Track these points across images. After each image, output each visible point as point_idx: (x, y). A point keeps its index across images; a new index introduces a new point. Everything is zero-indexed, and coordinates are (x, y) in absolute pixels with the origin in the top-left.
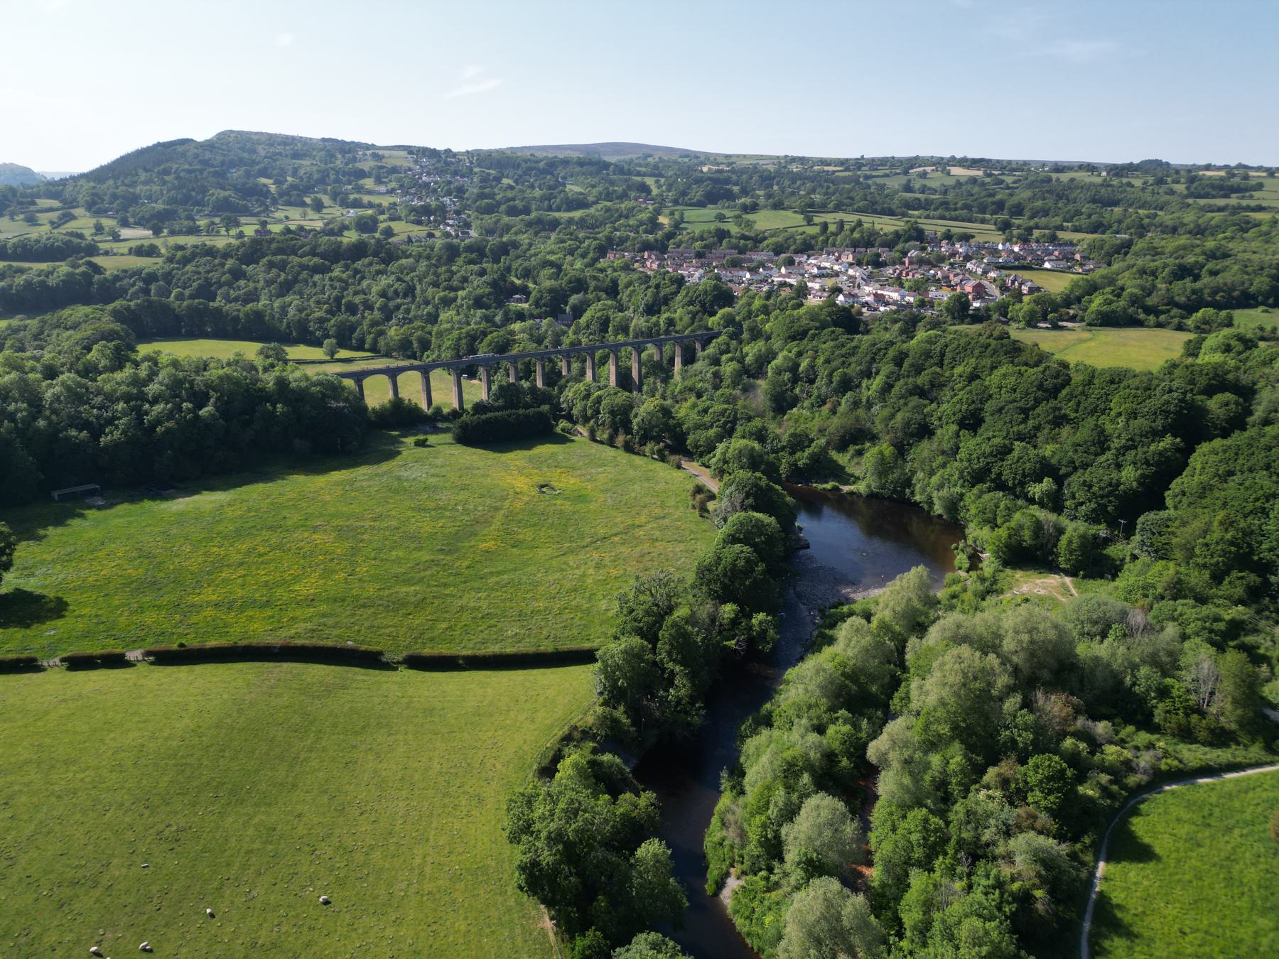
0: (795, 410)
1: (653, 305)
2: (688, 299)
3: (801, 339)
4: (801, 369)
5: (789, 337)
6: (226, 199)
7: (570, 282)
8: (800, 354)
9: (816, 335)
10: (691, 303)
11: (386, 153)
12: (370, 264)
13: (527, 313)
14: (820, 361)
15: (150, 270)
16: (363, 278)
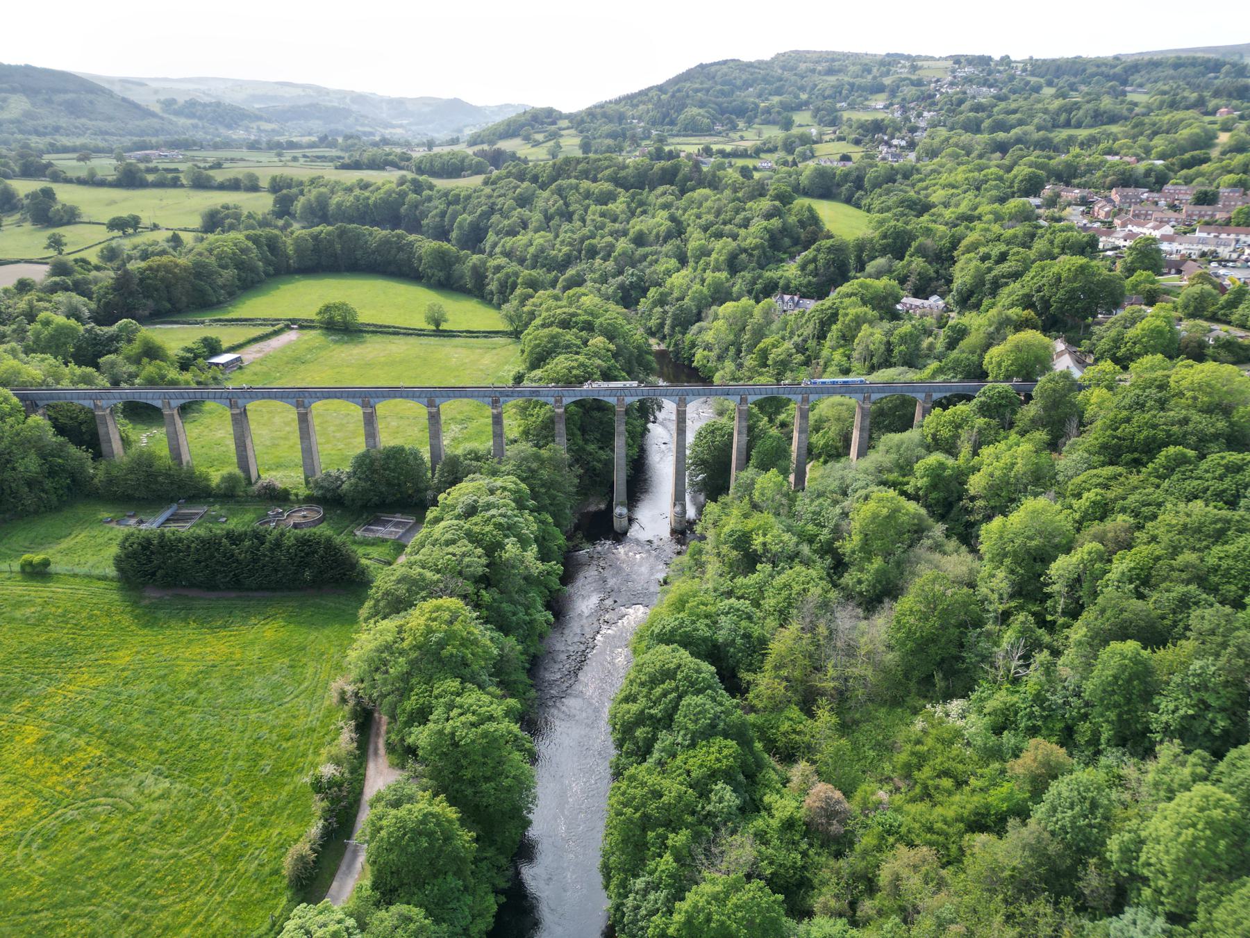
0: (956, 705)
1: (971, 293)
2: (1026, 290)
3: (1137, 463)
4: (1061, 567)
5: (1104, 447)
6: (693, 118)
7: (885, 236)
8: (1102, 511)
9: (1182, 460)
10: (1027, 303)
11: (926, 64)
12: (664, 193)
13: (782, 282)
14: (1121, 565)
15: (456, 192)
16: (644, 212)
